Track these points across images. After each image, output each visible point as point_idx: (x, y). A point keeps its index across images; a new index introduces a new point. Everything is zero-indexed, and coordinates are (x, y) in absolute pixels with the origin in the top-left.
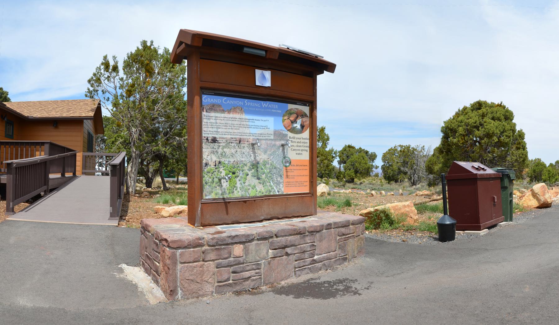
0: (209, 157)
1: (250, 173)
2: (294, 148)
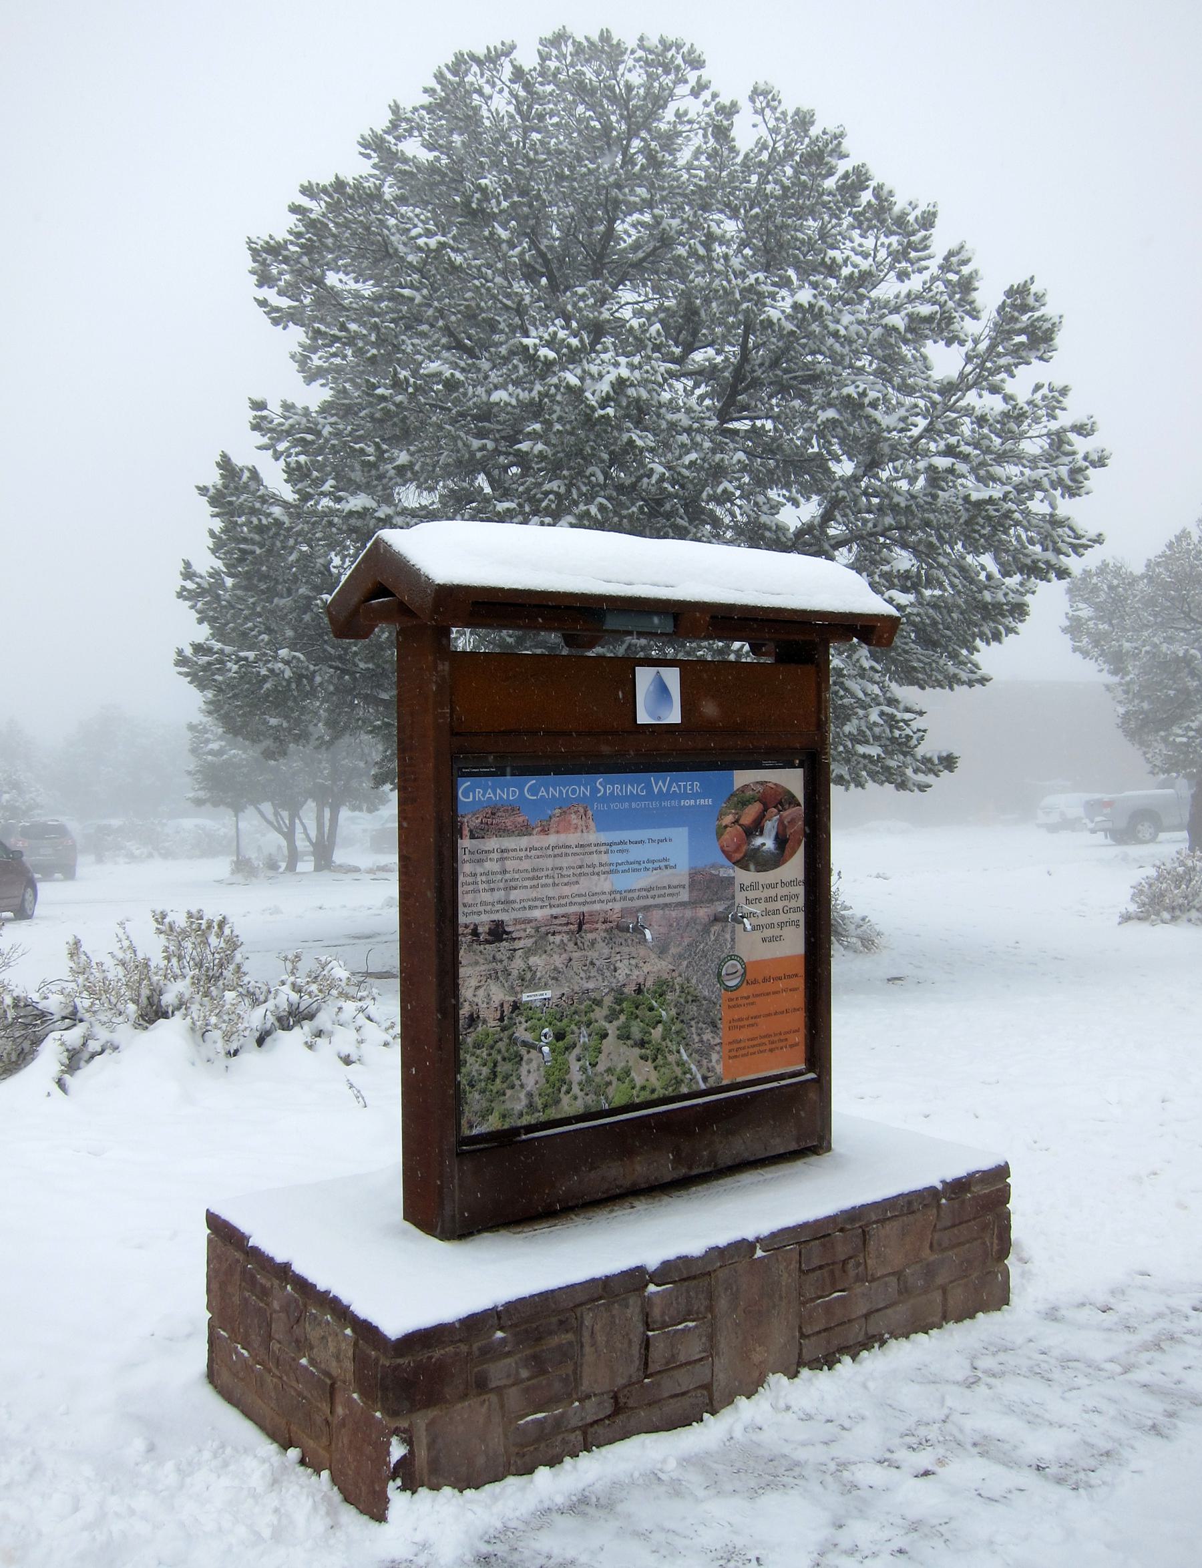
0: (481, 992)
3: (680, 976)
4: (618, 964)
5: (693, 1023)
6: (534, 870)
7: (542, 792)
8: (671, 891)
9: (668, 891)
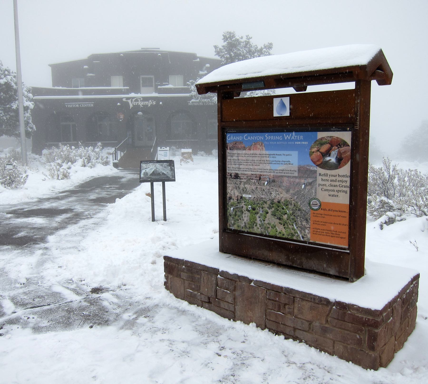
0: (232, 191)
1: (270, 211)
2: (325, 188)
3: (294, 200)
4: (272, 192)
5: (298, 217)
6: (246, 160)
7: (249, 138)
8: (291, 172)
9: (290, 172)
